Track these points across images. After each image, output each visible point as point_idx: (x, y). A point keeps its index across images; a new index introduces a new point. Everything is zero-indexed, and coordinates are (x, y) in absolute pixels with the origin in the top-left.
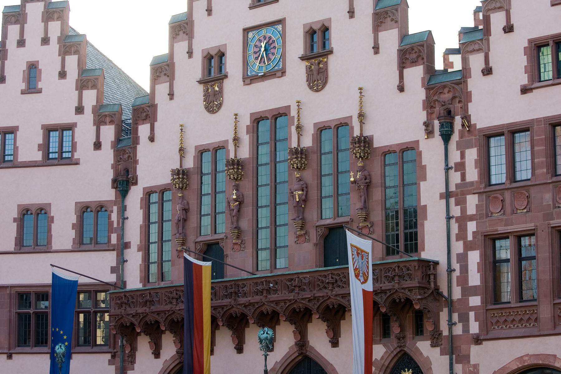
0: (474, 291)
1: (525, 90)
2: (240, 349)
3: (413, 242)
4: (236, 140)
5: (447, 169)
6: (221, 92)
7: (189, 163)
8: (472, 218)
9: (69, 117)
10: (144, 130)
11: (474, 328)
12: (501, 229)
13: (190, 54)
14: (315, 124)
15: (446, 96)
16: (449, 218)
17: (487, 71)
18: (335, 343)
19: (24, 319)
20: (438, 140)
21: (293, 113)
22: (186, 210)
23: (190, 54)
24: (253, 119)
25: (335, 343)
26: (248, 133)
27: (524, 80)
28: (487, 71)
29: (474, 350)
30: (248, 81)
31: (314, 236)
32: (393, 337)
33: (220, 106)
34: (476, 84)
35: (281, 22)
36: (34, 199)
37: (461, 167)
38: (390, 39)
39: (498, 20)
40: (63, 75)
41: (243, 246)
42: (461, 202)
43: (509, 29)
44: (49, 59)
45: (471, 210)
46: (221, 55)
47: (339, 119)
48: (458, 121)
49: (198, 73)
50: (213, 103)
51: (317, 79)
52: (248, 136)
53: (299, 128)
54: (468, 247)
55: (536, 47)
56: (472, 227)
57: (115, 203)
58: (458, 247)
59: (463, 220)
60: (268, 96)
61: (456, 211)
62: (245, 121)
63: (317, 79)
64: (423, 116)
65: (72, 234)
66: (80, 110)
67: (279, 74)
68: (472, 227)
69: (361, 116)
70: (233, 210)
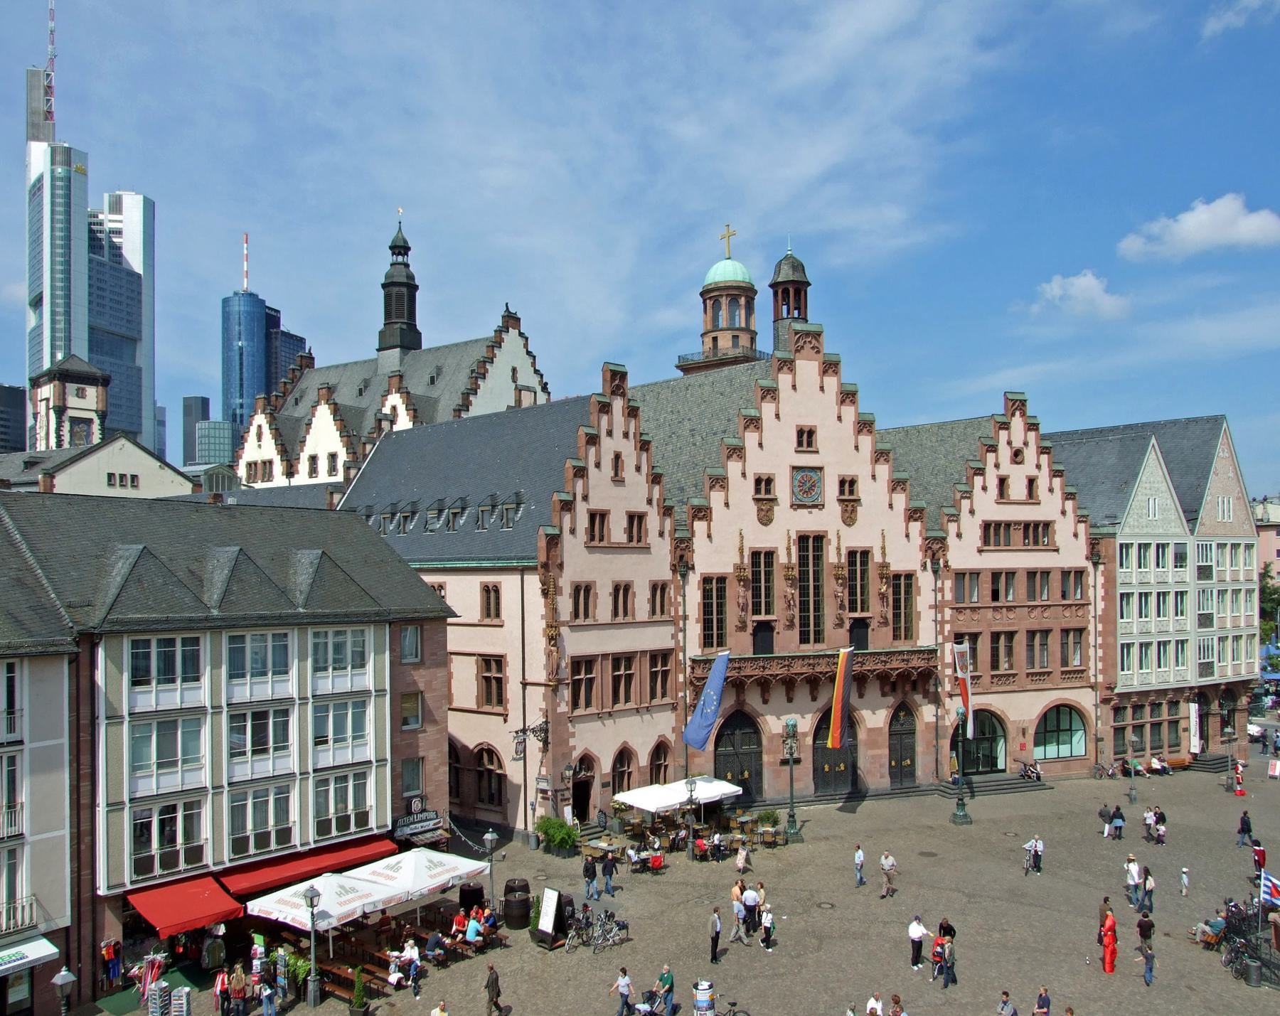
0: (947, 666)
1: (980, 551)
2: (790, 700)
3: (909, 634)
4: (789, 549)
5: (935, 591)
6: (771, 510)
7: (746, 561)
8: (947, 622)
9: (641, 507)
10: (699, 526)
11: (948, 687)
12: (964, 630)
13: (744, 475)
15: (936, 547)
16: (935, 621)
17: (959, 535)
18: (861, 696)
19: (616, 680)
20: (929, 574)
21: (832, 536)
23: (744, 475)
25: (861, 696)
27: (979, 543)
28: (959, 535)
29: (947, 700)
32: (899, 691)
33: (770, 521)
34: (952, 540)
35: (821, 469)
36: (623, 577)
37: (942, 590)
38: (900, 500)
39: (965, 504)
40: (638, 469)
42: (942, 612)
43: (972, 512)
44: (628, 450)
45: (947, 617)
46: (769, 481)
48: (941, 562)
50: (765, 518)
51: (849, 517)
53: (838, 549)
54: (946, 640)
55: (986, 526)
56: (947, 627)
57: (672, 581)
58: (940, 639)
59: (943, 622)
61: (939, 618)
62: (794, 536)
63: (849, 517)
64: (920, 555)
65: (647, 607)
66: (650, 502)
68: (947, 627)
69: (883, 548)
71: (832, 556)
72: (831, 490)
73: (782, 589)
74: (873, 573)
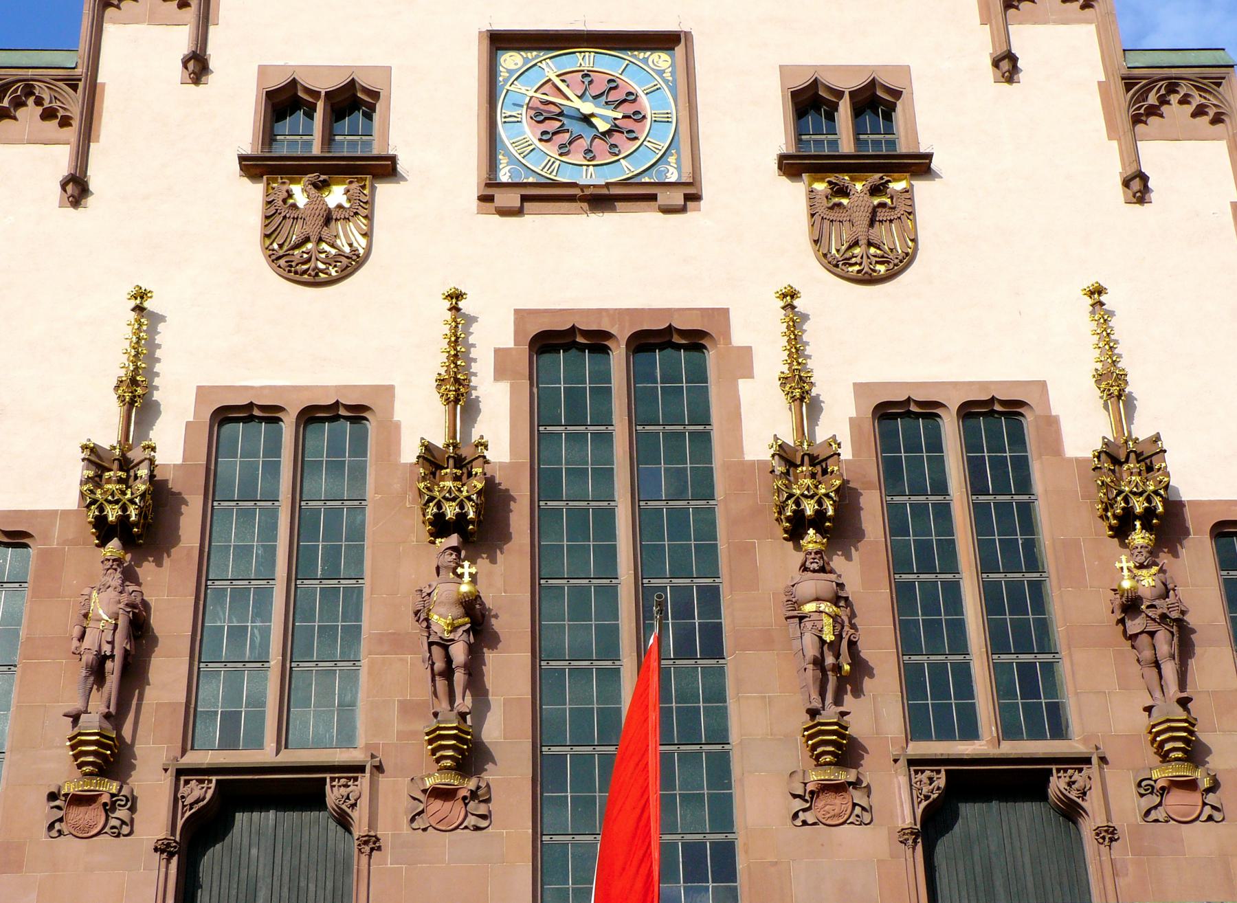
13: (197, 66)
14: (861, 389)
21: (756, 331)
22: (139, 626)
23: (197, 66)
24: (534, 330)
26: (501, 372)
30: (511, 199)
31: (897, 799)
33: (352, 263)
41: (482, 809)
47: (983, 385)
49: (245, 138)
52: (504, 387)
60: (609, 268)
67: (677, 198)
70: (445, 645)
71: (757, 421)
72: (744, 133)
73: (402, 570)
74: (1064, 517)
